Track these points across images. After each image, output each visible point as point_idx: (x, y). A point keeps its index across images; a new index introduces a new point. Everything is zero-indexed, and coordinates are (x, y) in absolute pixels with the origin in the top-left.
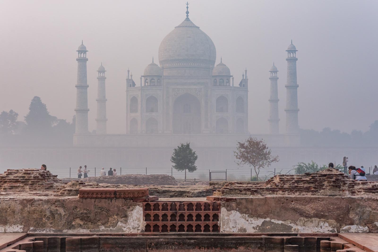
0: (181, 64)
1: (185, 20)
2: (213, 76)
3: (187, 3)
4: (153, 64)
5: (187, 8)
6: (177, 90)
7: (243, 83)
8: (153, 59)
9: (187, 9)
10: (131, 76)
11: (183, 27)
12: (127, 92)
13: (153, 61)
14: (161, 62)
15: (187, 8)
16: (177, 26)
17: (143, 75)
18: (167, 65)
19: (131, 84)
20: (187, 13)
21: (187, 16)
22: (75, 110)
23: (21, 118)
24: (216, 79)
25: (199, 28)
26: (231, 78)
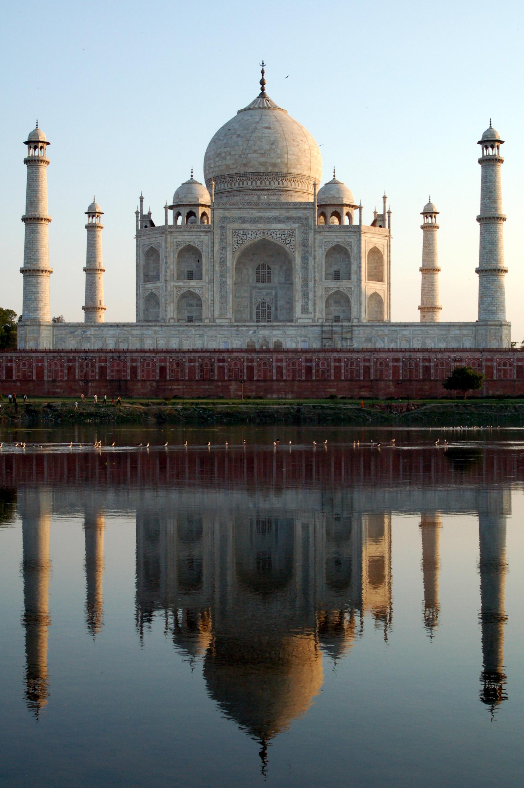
0: (250, 183)
1: (258, 97)
3: (263, 63)
4: (191, 183)
5: (263, 72)
6: (242, 232)
8: (192, 172)
9: (263, 75)
12: (137, 240)
13: (192, 176)
14: (208, 182)
15: (263, 72)
16: (243, 108)
17: (170, 203)
18: (222, 187)
19: (145, 222)
20: (262, 82)
21: (263, 89)
22: (83, 309)
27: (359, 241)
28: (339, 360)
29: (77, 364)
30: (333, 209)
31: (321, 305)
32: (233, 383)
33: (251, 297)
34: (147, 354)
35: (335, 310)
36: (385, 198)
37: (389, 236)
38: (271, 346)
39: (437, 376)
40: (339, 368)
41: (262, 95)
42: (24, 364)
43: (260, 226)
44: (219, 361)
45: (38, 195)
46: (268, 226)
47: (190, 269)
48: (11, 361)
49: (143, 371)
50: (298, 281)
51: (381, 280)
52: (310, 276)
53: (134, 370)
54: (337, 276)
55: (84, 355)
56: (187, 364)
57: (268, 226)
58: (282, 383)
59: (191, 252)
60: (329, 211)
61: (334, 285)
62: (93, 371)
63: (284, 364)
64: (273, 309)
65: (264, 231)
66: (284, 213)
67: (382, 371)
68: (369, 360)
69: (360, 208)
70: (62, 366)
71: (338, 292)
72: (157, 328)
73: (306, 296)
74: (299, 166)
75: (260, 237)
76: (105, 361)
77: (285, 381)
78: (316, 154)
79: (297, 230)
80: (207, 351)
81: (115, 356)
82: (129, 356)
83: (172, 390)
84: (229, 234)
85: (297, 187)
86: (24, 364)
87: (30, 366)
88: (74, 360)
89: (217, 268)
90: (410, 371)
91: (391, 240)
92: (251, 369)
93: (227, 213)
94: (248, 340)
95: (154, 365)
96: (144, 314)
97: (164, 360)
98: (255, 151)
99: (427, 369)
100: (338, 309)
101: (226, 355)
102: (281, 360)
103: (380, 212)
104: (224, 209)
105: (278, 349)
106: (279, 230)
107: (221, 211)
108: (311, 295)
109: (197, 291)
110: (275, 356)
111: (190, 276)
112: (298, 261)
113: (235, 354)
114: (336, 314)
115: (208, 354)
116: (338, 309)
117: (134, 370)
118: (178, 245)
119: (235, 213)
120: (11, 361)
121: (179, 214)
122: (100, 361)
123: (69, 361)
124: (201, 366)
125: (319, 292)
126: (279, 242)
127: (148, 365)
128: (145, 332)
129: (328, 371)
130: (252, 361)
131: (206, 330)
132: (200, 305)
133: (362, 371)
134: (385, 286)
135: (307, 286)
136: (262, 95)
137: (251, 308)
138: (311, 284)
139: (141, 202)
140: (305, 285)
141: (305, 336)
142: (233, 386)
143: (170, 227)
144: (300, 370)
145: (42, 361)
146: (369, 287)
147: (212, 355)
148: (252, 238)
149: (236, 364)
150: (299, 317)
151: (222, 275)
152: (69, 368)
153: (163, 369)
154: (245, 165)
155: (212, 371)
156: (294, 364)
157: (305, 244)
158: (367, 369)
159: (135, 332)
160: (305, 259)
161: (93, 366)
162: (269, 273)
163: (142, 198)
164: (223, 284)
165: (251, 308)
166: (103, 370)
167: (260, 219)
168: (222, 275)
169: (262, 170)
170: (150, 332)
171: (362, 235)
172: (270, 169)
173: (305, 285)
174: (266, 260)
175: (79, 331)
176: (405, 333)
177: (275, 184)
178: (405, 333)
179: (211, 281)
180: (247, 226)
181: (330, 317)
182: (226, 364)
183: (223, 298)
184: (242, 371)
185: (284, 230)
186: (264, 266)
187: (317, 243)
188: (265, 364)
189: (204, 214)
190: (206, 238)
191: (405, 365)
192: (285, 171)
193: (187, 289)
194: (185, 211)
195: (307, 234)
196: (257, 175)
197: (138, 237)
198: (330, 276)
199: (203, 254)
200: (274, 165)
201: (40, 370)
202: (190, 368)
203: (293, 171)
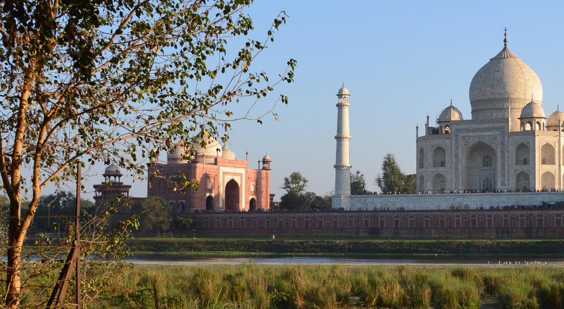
5: (505, 34)
15: (505, 34)
20: (505, 41)
21: (505, 45)
27: (534, 140)
28: (490, 216)
29: (354, 219)
30: (528, 120)
31: (513, 180)
32: (433, 230)
33: (480, 175)
34: (389, 213)
35: (523, 183)
38: (463, 208)
39: (546, 225)
40: (491, 220)
42: (328, 219)
43: (478, 134)
44: (426, 217)
45: (507, 91)
46: (481, 134)
47: (442, 160)
48: (321, 217)
49: (386, 223)
50: (499, 166)
51: (554, 164)
52: (506, 163)
53: (382, 221)
54: (525, 162)
55: (357, 214)
56: (409, 219)
57: (481, 134)
58: (459, 230)
61: (520, 168)
62: (362, 223)
63: (461, 219)
64: (493, 182)
65: (480, 137)
66: (491, 125)
67: (514, 222)
68: (507, 216)
70: (346, 220)
71: (523, 172)
72: (402, 198)
73: (503, 175)
74: (516, 93)
75: (477, 140)
76: (367, 217)
77: (461, 228)
78: (531, 84)
79: (498, 136)
80: (419, 211)
81: (372, 214)
82: (379, 214)
83: (402, 233)
84: (460, 139)
85: (516, 106)
86: (328, 219)
87: (331, 220)
88: (352, 217)
89: (454, 160)
90: (531, 222)
91: (561, 138)
92: (442, 221)
93: (459, 127)
94: (450, 204)
95: (392, 220)
96: (420, 187)
97: (397, 217)
98: (488, 86)
99: (540, 221)
100: (525, 182)
101: (429, 213)
102: (459, 216)
104: (457, 125)
105: (467, 210)
107: (456, 126)
108: (506, 175)
109: (443, 174)
110: (456, 214)
111: (443, 164)
112: (499, 154)
113: (434, 213)
114: (525, 185)
115: (420, 213)
116: (525, 182)
117: (382, 221)
118: (433, 147)
119: (464, 126)
120: (321, 217)
122: (365, 217)
123: (350, 217)
124: (417, 220)
125: (512, 172)
126: (488, 143)
127: (389, 219)
128: (396, 200)
129: (485, 222)
130: (443, 217)
131: (428, 198)
132: (444, 181)
133: (503, 223)
134: (556, 167)
135: (504, 169)
136: (505, 48)
137: (480, 182)
138: (506, 168)
139: (428, 119)
140: (503, 169)
141: (482, 201)
142: (433, 232)
144: (469, 222)
145: (336, 217)
146: (540, 169)
147: (422, 213)
148: (473, 141)
149: (434, 218)
150: (500, 187)
151: (457, 164)
152: (350, 221)
153: (397, 222)
154: (483, 95)
155: (422, 223)
156: (466, 218)
157: (503, 144)
158: (506, 221)
159: (391, 200)
160: (503, 153)
161: (362, 220)
162: (491, 161)
163: (428, 117)
164: (457, 169)
165: (480, 182)
166: (366, 222)
167: (477, 130)
168: (457, 164)
169: (493, 97)
170: (399, 200)
171: (536, 137)
172: (497, 96)
173: (503, 169)
175: (363, 200)
176: (538, 198)
177: (500, 105)
178: (538, 198)
179: (451, 167)
180: (470, 134)
181: (522, 187)
182: (429, 219)
183: (457, 177)
184: (438, 223)
185: (491, 136)
186: (487, 156)
187: (510, 143)
188: (450, 218)
190: (448, 142)
191: (527, 218)
192: (507, 97)
193: (437, 173)
195: (504, 137)
196: (490, 100)
197: (417, 141)
198: (521, 163)
199: (446, 151)
200: (500, 94)
201: (336, 222)
202: (412, 222)
203: (512, 96)
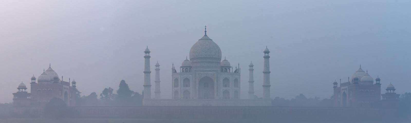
2: (221, 67)
4: (187, 60)
5: (206, 29)
7: (237, 71)
10: (174, 67)
11: (204, 39)
14: (191, 59)
15: (206, 29)
17: (181, 66)
19: (174, 71)
20: (206, 32)
21: (206, 33)
23: (115, 92)
24: (222, 69)
25: (212, 40)
26: (231, 68)
36: (239, 64)
37: (240, 75)
41: (206, 35)
54: (226, 86)
59: (186, 80)
60: (224, 68)
69: (232, 68)
103: (237, 68)
106: (211, 74)
121: (183, 69)
136: (206, 35)
143: (181, 73)
174: (206, 82)
189: (190, 69)
194: (185, 68)
